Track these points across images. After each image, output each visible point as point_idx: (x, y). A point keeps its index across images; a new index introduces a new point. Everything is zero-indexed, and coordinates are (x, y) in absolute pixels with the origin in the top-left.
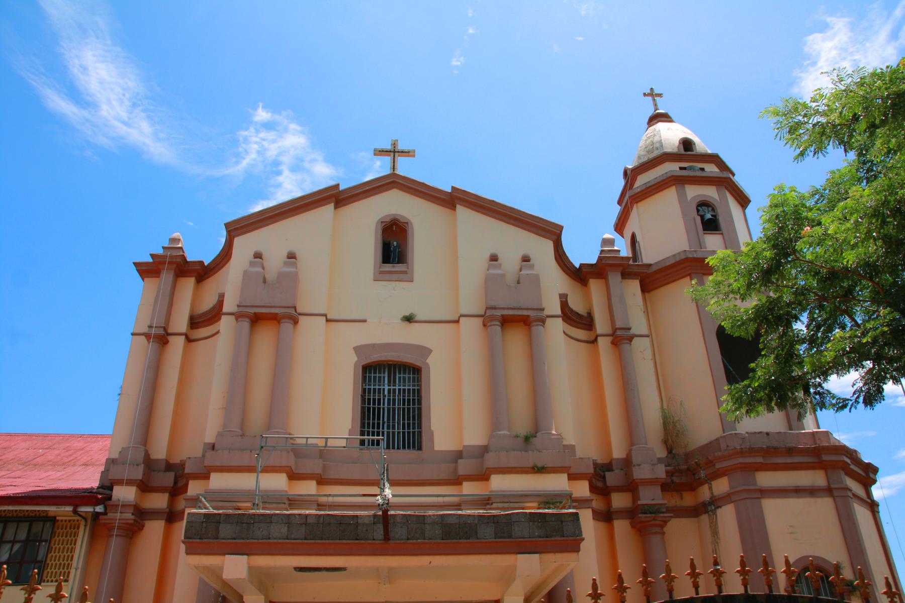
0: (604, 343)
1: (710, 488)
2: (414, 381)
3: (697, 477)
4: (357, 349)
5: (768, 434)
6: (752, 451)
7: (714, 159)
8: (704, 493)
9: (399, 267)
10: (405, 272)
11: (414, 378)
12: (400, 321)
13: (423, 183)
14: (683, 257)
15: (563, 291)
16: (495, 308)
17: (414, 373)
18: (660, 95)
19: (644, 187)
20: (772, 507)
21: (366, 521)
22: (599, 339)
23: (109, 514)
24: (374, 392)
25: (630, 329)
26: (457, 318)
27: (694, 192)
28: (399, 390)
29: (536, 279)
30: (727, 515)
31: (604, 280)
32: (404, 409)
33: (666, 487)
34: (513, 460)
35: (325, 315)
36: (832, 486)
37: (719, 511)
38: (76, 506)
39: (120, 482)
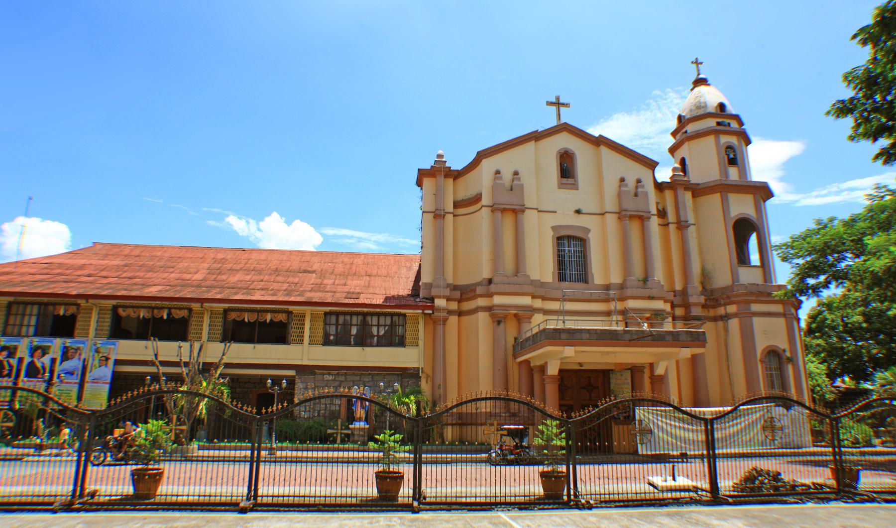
0: (672, 227)
1: (725, 309)
3: (718, 303)
4: (554, 228)
5: (758, 285)
6: (751, 294)
7: (737, 118)
8: (721, 311)
9: (570, 181)
10: (574, 184)
12: (573, 213)
14: (719, 183)
15: (659, 201)
18: (701, 63)
19: (695, 133)
21: (621, 332)
22: (670, 225)
25: (687, 221)
27: (725, 139)
30: (734, 324)
34: (640, 292)
35: (537, 209)
36: (787, 313)
38: (423, 310)
39: (439, 297)
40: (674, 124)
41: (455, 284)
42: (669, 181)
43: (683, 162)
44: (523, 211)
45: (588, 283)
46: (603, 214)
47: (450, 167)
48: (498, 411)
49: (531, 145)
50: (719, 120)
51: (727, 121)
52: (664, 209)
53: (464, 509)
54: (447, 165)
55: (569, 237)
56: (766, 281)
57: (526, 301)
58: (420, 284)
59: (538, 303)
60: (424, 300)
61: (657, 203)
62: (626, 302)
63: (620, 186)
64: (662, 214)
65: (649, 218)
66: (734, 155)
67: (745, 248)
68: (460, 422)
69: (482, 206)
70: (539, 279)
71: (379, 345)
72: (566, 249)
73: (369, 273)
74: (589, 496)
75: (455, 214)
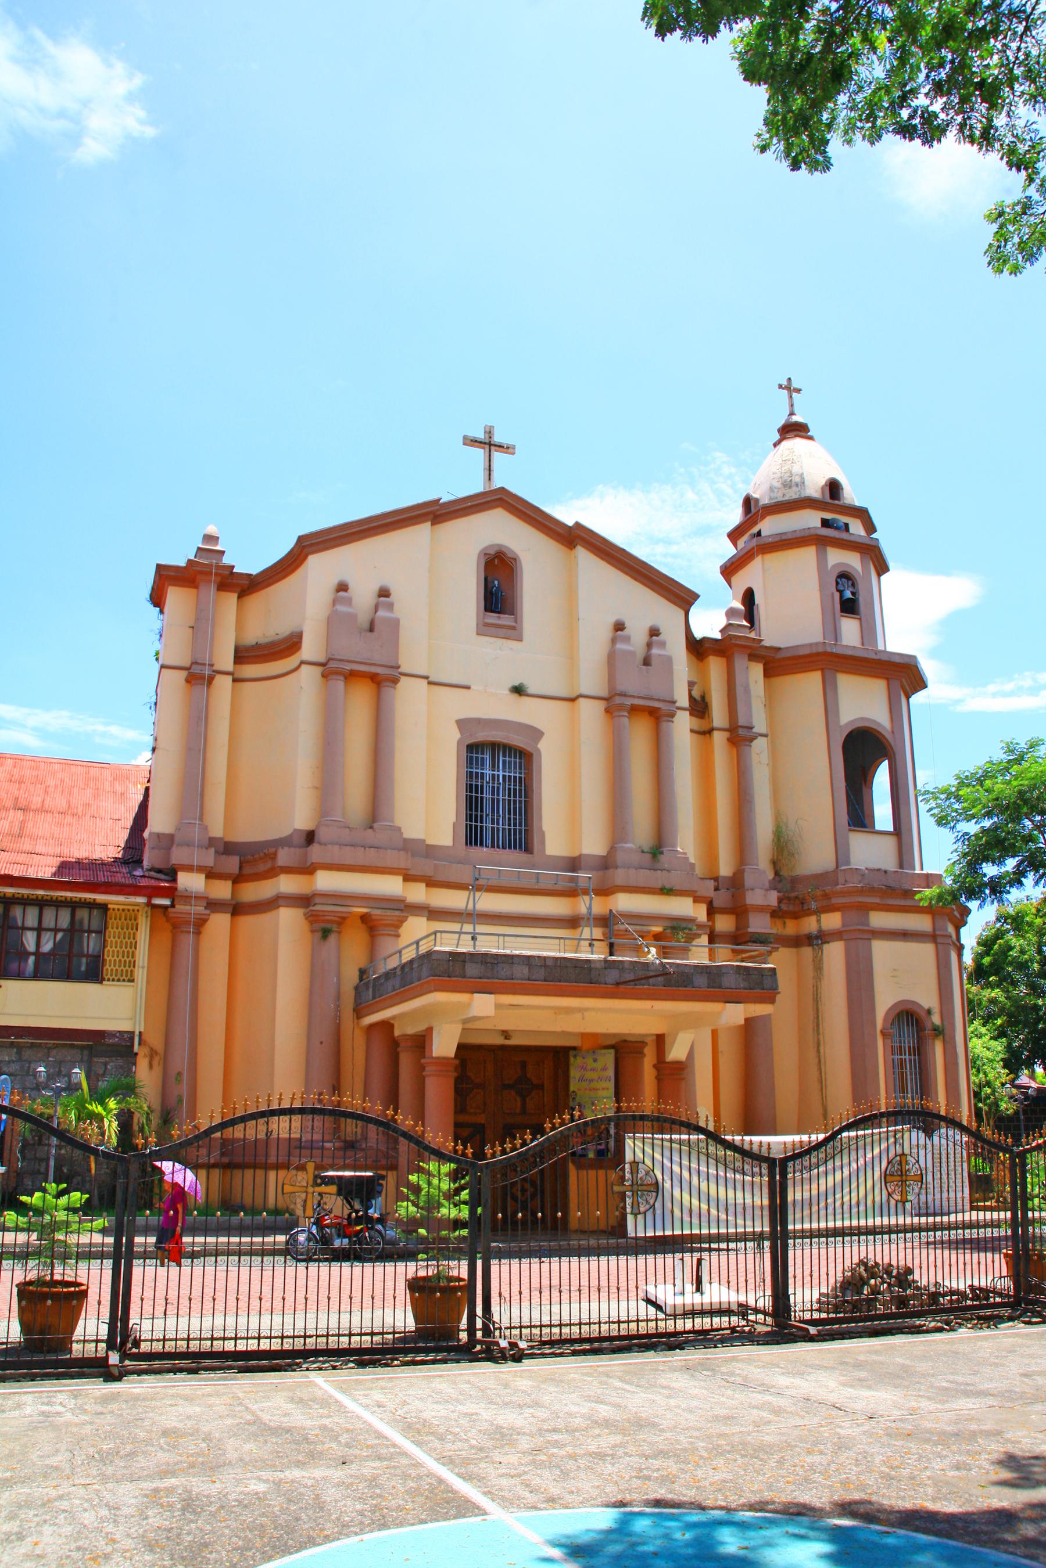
0: (719, 739)
1: (819, 921)
2: (520, 768)
3: (805, 907)
4: (462, 724)
5: (886, 872)
6: (871, 890)
7: (862, 514)
8: (810, 925)
9: (506, 620)
10: (513, 628)
11: (520, 763)
12: (507, 692)
13: (538, 508)
14: (820, 650)
16: (625, 695)
17: (520, 758)
18: (798, 391)
19: (777, 539)
20: (880, 949)
21: (598, 966)
22: (716, 734)
23: (177, 906)
24: (477, 777)
25: (752, 728)
26: (574, 695)
27: (837, 558)
28: (504, 776)
29: (668, 661)
30: (835, 953)
31: (724, 660)
32: (509, 801)
33: (776, 914)
34: (644, 877)
35: (427, 678)
36: (938, 933)
37: (825, 947)
38: (150, 898)
39: (189, 868)
40: (735, 516)
41: (227, 839)
42: (718, 636)
43: (749, 598)
44: (395, 681)
45: (531, 853)
46: (573, 700)
47: (233, 567)
48: (317, 1137)
49: (423, 531)
50: (828, 516)
51: (843, 519)
52: (703, 697)
53: (230, 1368)
54: (226, 560)
55: (495, 747)
56: (901, 866)
57: (391, 886)
58: (146, 835)
59: (417, 894)
60: (153, 874)
61: (691, 684)
62: (612, 898)
63: (614, 641)
64: (699, 707)
65: (672, 715)
66: (853, 594)
67: (865, 790)
68: (225, 1160)
69: (302, 663)
70: (421, 836)
71: (38, 975)
72: (488, 772)
73: (22, 803)
74: (516, 1332)
75: (236, 676)
